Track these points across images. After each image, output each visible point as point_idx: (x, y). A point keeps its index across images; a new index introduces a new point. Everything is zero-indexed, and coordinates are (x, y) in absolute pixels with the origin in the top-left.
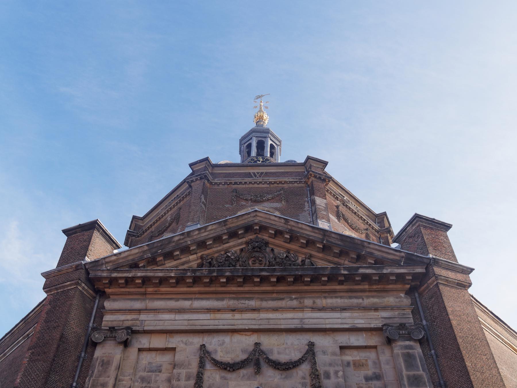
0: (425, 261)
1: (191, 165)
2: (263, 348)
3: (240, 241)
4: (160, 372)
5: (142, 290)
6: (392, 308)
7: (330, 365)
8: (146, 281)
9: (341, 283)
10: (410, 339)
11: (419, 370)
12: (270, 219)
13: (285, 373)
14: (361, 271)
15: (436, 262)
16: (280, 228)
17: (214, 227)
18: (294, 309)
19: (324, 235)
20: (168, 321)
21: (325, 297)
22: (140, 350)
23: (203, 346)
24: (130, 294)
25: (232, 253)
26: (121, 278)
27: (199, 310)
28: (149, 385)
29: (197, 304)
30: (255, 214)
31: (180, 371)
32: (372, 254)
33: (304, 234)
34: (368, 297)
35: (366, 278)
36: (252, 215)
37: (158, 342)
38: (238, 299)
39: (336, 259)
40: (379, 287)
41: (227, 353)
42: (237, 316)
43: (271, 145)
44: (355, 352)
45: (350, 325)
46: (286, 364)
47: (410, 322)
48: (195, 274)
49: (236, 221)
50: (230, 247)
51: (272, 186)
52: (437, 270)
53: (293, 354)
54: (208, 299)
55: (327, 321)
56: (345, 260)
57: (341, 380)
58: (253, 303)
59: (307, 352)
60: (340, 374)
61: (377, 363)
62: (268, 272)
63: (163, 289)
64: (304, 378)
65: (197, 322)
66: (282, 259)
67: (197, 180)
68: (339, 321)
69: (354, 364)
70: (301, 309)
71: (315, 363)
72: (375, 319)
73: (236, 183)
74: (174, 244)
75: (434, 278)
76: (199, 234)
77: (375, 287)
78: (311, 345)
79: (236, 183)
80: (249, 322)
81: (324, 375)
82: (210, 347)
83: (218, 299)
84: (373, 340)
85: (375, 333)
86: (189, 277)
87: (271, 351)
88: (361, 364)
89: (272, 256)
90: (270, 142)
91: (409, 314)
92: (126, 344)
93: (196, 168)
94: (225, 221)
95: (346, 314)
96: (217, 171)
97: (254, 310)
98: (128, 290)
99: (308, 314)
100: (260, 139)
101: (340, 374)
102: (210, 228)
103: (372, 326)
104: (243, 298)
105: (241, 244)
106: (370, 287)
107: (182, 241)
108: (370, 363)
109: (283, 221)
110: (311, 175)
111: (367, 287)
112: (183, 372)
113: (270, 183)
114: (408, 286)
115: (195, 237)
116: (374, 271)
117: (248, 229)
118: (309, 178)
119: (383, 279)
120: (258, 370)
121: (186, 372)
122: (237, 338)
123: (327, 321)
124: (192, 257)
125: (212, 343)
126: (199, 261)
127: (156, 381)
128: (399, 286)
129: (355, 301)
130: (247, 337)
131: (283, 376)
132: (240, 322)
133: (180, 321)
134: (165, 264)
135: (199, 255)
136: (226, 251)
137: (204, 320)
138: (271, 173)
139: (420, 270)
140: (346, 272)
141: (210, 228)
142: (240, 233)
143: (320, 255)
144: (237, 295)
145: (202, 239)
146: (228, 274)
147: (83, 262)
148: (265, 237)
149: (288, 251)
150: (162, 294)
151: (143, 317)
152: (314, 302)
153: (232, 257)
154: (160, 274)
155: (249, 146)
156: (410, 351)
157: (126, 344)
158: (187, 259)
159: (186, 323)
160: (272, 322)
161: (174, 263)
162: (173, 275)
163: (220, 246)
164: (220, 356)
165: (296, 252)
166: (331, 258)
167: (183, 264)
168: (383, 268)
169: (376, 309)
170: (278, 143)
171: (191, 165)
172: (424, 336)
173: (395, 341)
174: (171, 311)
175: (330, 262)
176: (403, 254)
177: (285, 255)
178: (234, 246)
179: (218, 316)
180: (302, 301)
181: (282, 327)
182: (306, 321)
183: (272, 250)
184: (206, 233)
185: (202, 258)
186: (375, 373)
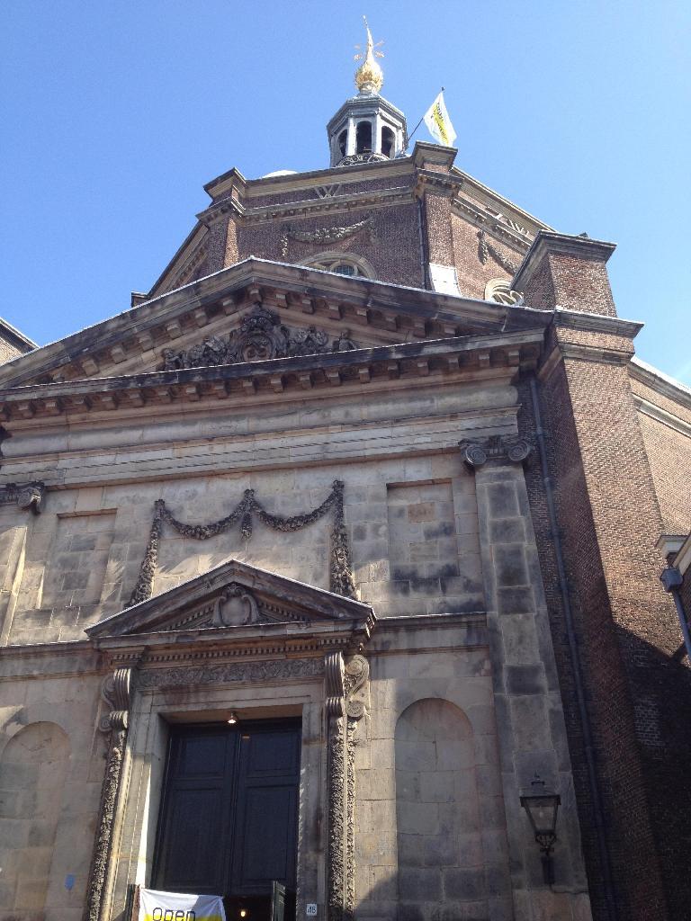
0: (544, 319)
1: (207, 188)
2: (259, 496)
3: (230, 318)
4: (92, 549)
5: (61, 419)
6: (483, 411)
8: (63, 404)
9: (395, 375)
10: (507, 463)
11: (513, 512)
12: (276, 274)
13: (290, 537)
14: (428, 351)
15: (564, 320)
16: (293, 289)
17: (179, 297)
19: (369, 294)
20: (105, 465)
21: (368, 404)
22: (61, 517)
23: (160, 502)
24: (41, 427)
25: (216, 342)
26: (21, 402)
27: (164, 442)
28: (73, 571)
29: (151, 434)
30: (250, 268)
31: (120, 545)
32: (450, 317)
33: (333, 294)
34: (441, 396)
35: (435, 363)
36: (245, 269)
37: (88, 502)
38: (219, 419)
40: (462, 375)
42: (218, 448)
44: (413, 493)
45: (407, 447)
46: (291, 521)
47: (511, 432)
48: (142, 383)
49: (218, 282)
50: (214, 332)
51: (352, 210)
52: (564, 334)
53: (307, 505)
54: (168, 424)
56: (407, 334)
57: (383, 540)
58: (243, 425)
59: (331, 498)
60: (383, 529)
61: (449, 507)
62: (266, 369)
63: (95, 415)
64: (321, 541)
65: (150, 465)
66: (300, 344)
67: (216, 216)
68: (389, 442)
69: (410, 512)
70: (324, 427)
71: (340, 515)
72: (448, 434)
73: (287, 213)
74: (109, 335)
75: (557, 350)
76: (152, 313)
77: (454, 377)
78: (339, 486)
79: (287, 213)
80: (238, 457)
81: (354, 533)
82: (171, 504)
83: (185, 423)
85: (449, 456)
86: (134, 389)
87: (272, 501)
88: (422, 511)
90: (380, 124)
91: (512, 419)
92: (34, 510)
93: (218, 191)
94: (198, 285)
95: (401, 429)
96: (256, 193)
97: (245, 435)
99: (338, 434)
100: (362, 120)
101: (383, 529)
102: (170, 301)
103: (444, 445)
104: (228, 418)
105: (232, 324)
106: (446, 378)
107: (123, 330)
108: (438, 507)
109: (297, 274)
111: (440, 378)
112: (127, 546)
113: (349, 205)
114: (515, 370)
115: (146, 320)
116: (450, 349)
117: (240, 295)
118: (418, 188)
121: (131, 547)
122: (218, 484)
123: (367, 444)
124: (145, 356)
125: (175, 495)
126: (160, 360)
127: (85, 564)
128: (498, 371)
129: (417, 406)
130: (233, 482)
131: (288, 540)
133: (126, 464)
134: (99, 372)
135: (158, 350)
136: (207, 338)
137: (163, 459)
139: (534, 337)
140: (399, 356)
141: (170, 301)
142: (224, 304)
143: (367, 330)
144: (215, 416)
146: (197, 379)
148: (273, 308)
149: (313, 330)
150: (95, 423)
151: (64, 463)
152: (347, 414)
153: (216, 349)
154: (85, 390)
155: (344, 137)
156: (506, 483)
157: (34, 510)
158: (139, 359)
163: (194, 331)
164: (188, 516)
167: (132, 368)
168: (466, 341)
170: (399, 124)
171: (207, 188)
172: (530, 455)
173: (481, 466)
174: (107, 449)
176: (505, 312)
177: (306, 336)
178: (220, 329)
179: (187, 451)
180: (326, 414)
182: (332, 447)
183: (285, 330)
184: (165, 311)
186: (444, 524)
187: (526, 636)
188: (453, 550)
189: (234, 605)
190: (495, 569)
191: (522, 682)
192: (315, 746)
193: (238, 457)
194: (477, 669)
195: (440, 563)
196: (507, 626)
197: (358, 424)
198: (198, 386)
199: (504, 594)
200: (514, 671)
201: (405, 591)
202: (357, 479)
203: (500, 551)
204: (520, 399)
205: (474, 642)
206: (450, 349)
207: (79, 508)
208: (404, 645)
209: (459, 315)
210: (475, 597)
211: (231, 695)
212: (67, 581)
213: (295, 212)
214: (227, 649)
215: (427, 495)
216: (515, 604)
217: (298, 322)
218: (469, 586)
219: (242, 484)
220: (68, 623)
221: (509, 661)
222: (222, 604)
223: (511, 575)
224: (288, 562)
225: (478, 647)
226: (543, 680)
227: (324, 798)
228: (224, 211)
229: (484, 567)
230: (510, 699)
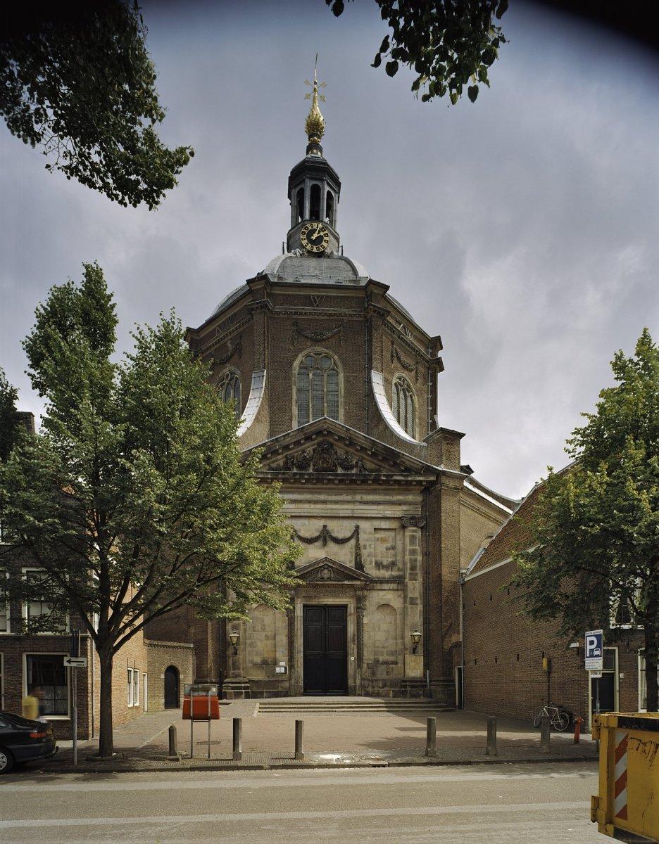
2: (328, 528)
7: (367, 540)
13: (341, 546)
14: (395, 478)
18: (348, 502)
21: (369, 494)
32: (404, 463)
34: (396, 494)
39: (379, 463)
41: (307, 531)
42: (313, 506)
43: (329, 192)
44: (383, 532)
46: (341, 540)
50: (306, 448)
51: (332, 318)
54: (293, 493)
55: (369, 512)
58: (322, 497)
60: (372, 546)
62: (333, 476)
71: (358, 540)
72: (397, 511)
73: (296, 313)
78: (357, 527)
80: (320, 511)
84: (394, 525)
89: (335, 457)
95: (381, 507)
96: (277, 291)
97: (325, 502)
103: (395, 516)
105: (314, 445)
108: (390, 539)
111: (397, 487)
114: (423, 488)
116: (403, 478)
118: (368, 313)
119: (408, 483)
120: (325, 544)
122: (313, 521)
123: (369, 512)
125: (297, 524)
128: (418, 487)
129: (388, 498)
132: (314, 511)
135: (284, 455)
138: (331, 297)
139: (432, 478)
140: (384, 478)
143: (368, 458)
144: (311, 492)
145: (285, 444)
148: (331, 440)
160: (334, 511)
161: (268, 462)
162: (269, 476)
164: (302, 534)
166: (375, 461)
169: (400, 504)
175: (374, 464)
179: (300, 506)
181: (341, 515)
185: (286, 456)
187: (415, 588)
188: (395, 555)
189: (326, 571)
190: (409, 565)
191: (413, 601)
192: (352, 616)
193: (320, 511)
194: (399, 596)
195: (390, 560)
196: (410, 584)
197: (366, 503)
198: (305, 479)
199: (410, 574)
200: (411, 598)
201: (379, 570)
202: (364, 525)
203: (411, 559)
204: (423, 501)
205: (399, 588)
206: (403, 478)
208: (379, 588)
209: (407, 462)
210: (401, 573)
211: (325, 600)
213: (301, 313)
214: (323, 586)
215: (388, 533)
216: (413, 578)
217: (341, 451)
218: (399, 570)
219: (322, 523)
221: (410, 595)
223: (413, 568)
225: (401, 590)
226: (419, 602)
227: (356, 630)
229: (404, 563)
230: (409, 606)
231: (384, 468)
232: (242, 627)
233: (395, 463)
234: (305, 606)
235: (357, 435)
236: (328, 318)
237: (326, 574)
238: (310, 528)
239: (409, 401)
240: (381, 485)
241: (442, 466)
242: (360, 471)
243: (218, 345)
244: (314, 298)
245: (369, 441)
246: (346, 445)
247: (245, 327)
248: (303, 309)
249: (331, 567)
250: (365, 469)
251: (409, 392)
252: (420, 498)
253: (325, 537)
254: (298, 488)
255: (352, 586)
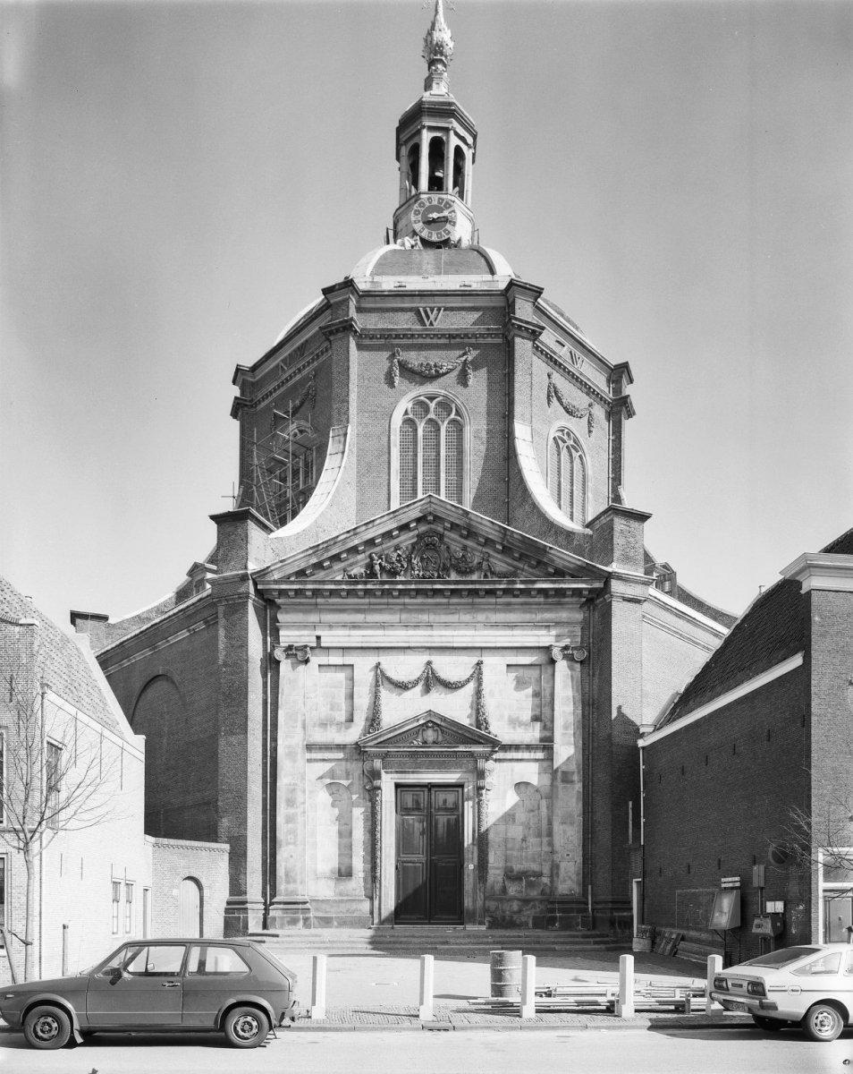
2: (434, 666)
3: (411, 534)
5: (314, 601)
24: (300, 604)
37: (335, 659)
39: (515, 563)
50: (401, 542)
54: (380, 611)
90: (454, 141)
98: (298, 600)
103: (541, 645)
105: (413, 537)
110: (514, 324)
111: (542, 600)
114: (585, 599)
119: (560, 593)
124: (360, 557)
128: (575, 599)
135: (368, 553)
136: (397, 548)
139: (598, 585)
143: (499, 556)
147: (249, 572)
148: (440, 529)
149: (465, 548)
152: (487, 618)
155: (415, 151)
159: (360, 639)
161: (342, 565)
165: (473, 549)
170: (470, 140)
175: (506, 563)
178: (406, 540)
181: (455, 645)
207: (331, 663)
209: (558, 561)
212: (331, 705)
214: (426, 754)
217: (454, 541)
219: (425, 658)
220: (339, 731)
222: (424, 730)
224: (456, 707)
228: (345, 329)
231: (523, 570)
232: (300, 819)
233: (539, 562)
234: (398, 786)
235: (479, 520)
236: (446, 341)
237: (430, 735)
238: (406, 667)
239: (577, 462)
240: (517, 596)
241: (614, 564)
242: (486, 576)
243: (282, 389)
244: (426, 312)
245: (497, 528)
246: (462, 536)
247: (321, 360)
248: (410, 329)
249: (438, 725)
250: (493, 573)
251: (577, 451)
252: (579, 616)
253: (431, 681)
254: (388, 604)
255: (471, 754)
